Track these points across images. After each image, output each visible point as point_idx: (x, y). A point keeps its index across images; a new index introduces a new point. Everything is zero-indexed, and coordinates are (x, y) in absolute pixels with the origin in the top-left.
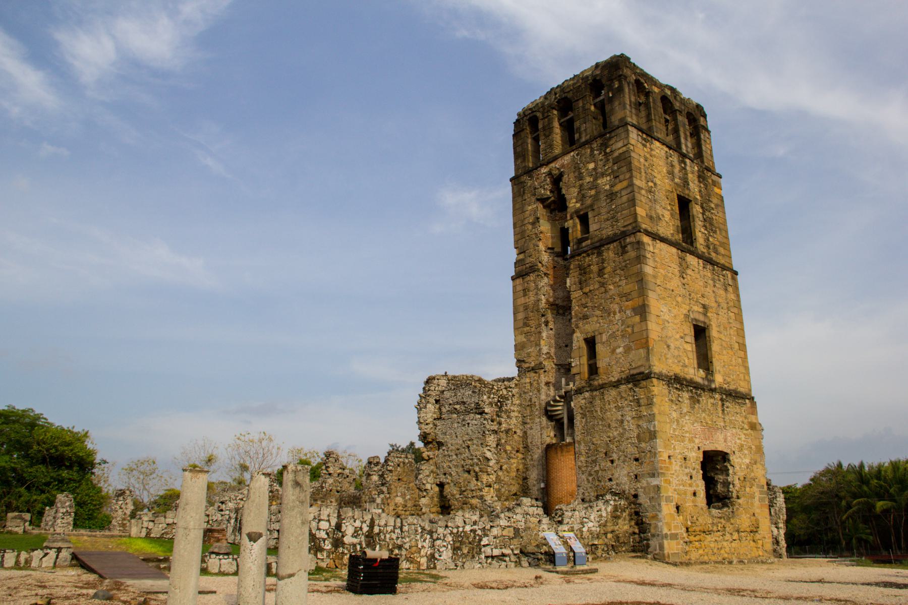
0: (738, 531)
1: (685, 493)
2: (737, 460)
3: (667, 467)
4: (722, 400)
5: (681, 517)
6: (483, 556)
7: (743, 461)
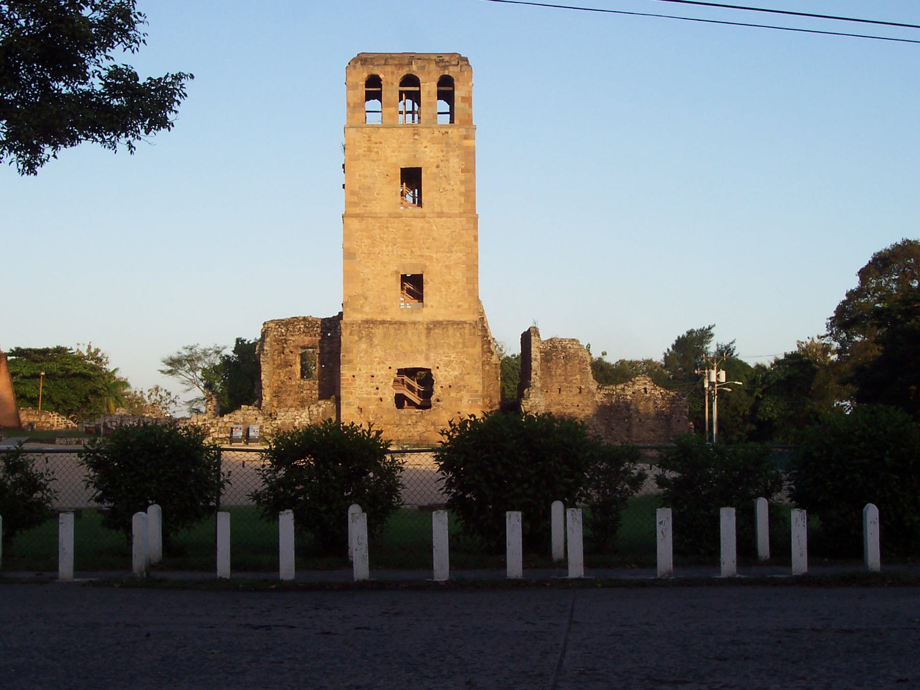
0: (433, 424)
1: (369, 399)
2: (442, 373)
3: (350, 383)
4: (429, 329)
5: (362, 416)
6: (211, 438)
7: (450, 373)
